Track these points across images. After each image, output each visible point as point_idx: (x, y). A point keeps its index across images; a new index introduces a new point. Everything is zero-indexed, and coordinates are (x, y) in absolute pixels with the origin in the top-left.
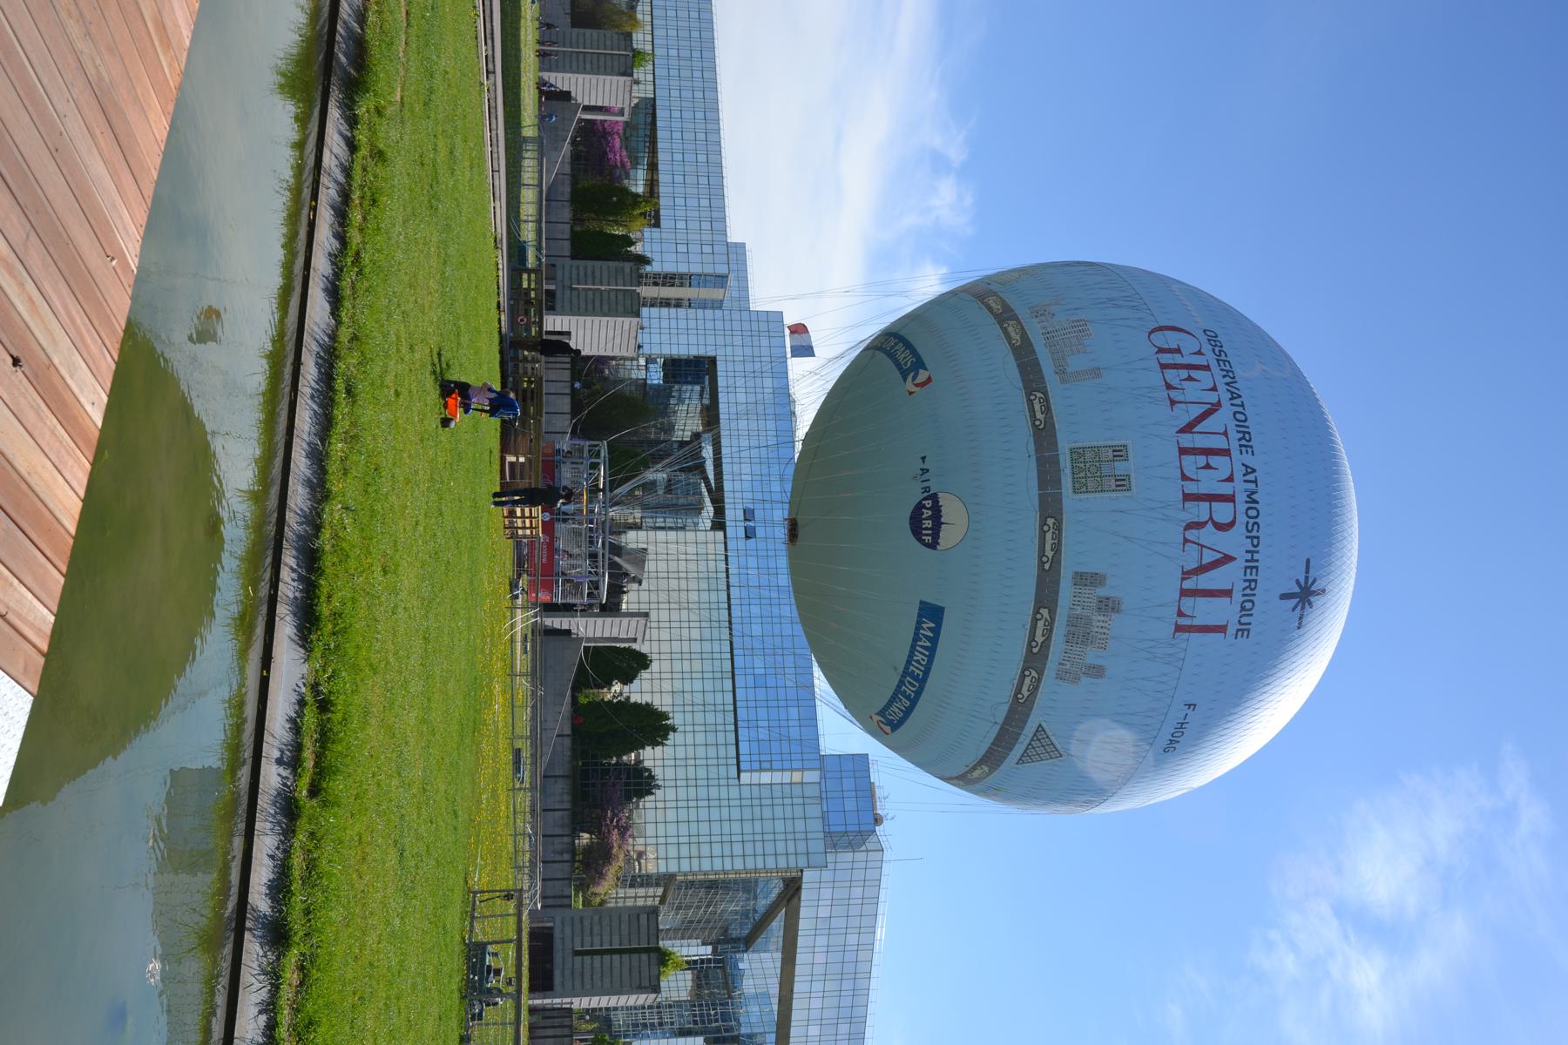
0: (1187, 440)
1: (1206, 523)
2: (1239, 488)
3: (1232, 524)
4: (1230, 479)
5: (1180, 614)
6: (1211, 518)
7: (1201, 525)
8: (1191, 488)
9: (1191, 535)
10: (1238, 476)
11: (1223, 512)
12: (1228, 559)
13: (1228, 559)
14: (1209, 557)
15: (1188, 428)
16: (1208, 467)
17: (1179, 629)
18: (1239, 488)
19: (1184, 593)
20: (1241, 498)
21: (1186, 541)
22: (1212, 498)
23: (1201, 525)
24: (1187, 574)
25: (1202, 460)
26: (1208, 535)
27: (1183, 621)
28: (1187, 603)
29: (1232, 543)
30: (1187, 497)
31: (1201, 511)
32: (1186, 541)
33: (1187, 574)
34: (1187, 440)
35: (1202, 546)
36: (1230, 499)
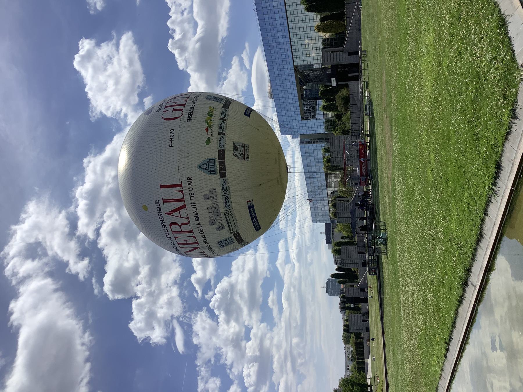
0: (196, 246)
1: (181, 225)
2: (172, 236)
3: (171, 225)
4: (176, 238)
5: (182, 192)
6: (180, 226)
7: (182, 224)
8: (191, 234)
9: (186, 221)
10: (173, 239)
11: (175, 228)
12: (170, 213)
13: (170, 213)
14: (177, 214)
15: (196, 248)
16: (186, 240)
17: (180, 185)
18: (172, 236)
19: (182, 200)
20: (170, 232)
21: (188, 218)
22: (181, 232)
23: (182, 224)
24: (184, 206)
25: (188, 242)
26: (180, 221)
27: (179, 189)
28: (179, 196)
29: (168, 219)
30: (191, 231)
31: (185, 228)
32: (188, 218)
33: (184, 206)
34: (196, 246)
35: (181, 217)
36: (174, 232)
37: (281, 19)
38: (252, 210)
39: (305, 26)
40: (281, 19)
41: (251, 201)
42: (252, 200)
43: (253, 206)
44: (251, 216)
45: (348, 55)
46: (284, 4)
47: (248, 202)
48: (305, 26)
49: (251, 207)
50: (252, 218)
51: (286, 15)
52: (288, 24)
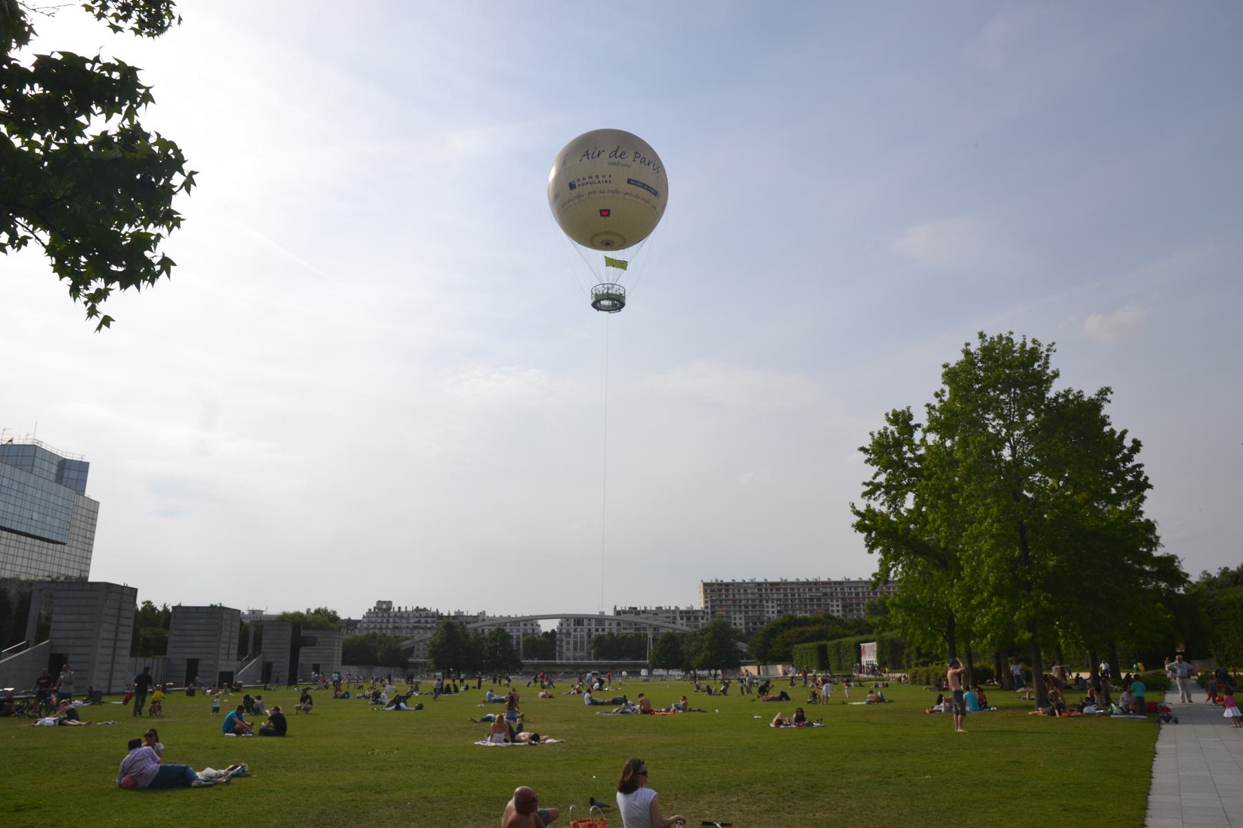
43: (655, 195)
50: (649, 187)
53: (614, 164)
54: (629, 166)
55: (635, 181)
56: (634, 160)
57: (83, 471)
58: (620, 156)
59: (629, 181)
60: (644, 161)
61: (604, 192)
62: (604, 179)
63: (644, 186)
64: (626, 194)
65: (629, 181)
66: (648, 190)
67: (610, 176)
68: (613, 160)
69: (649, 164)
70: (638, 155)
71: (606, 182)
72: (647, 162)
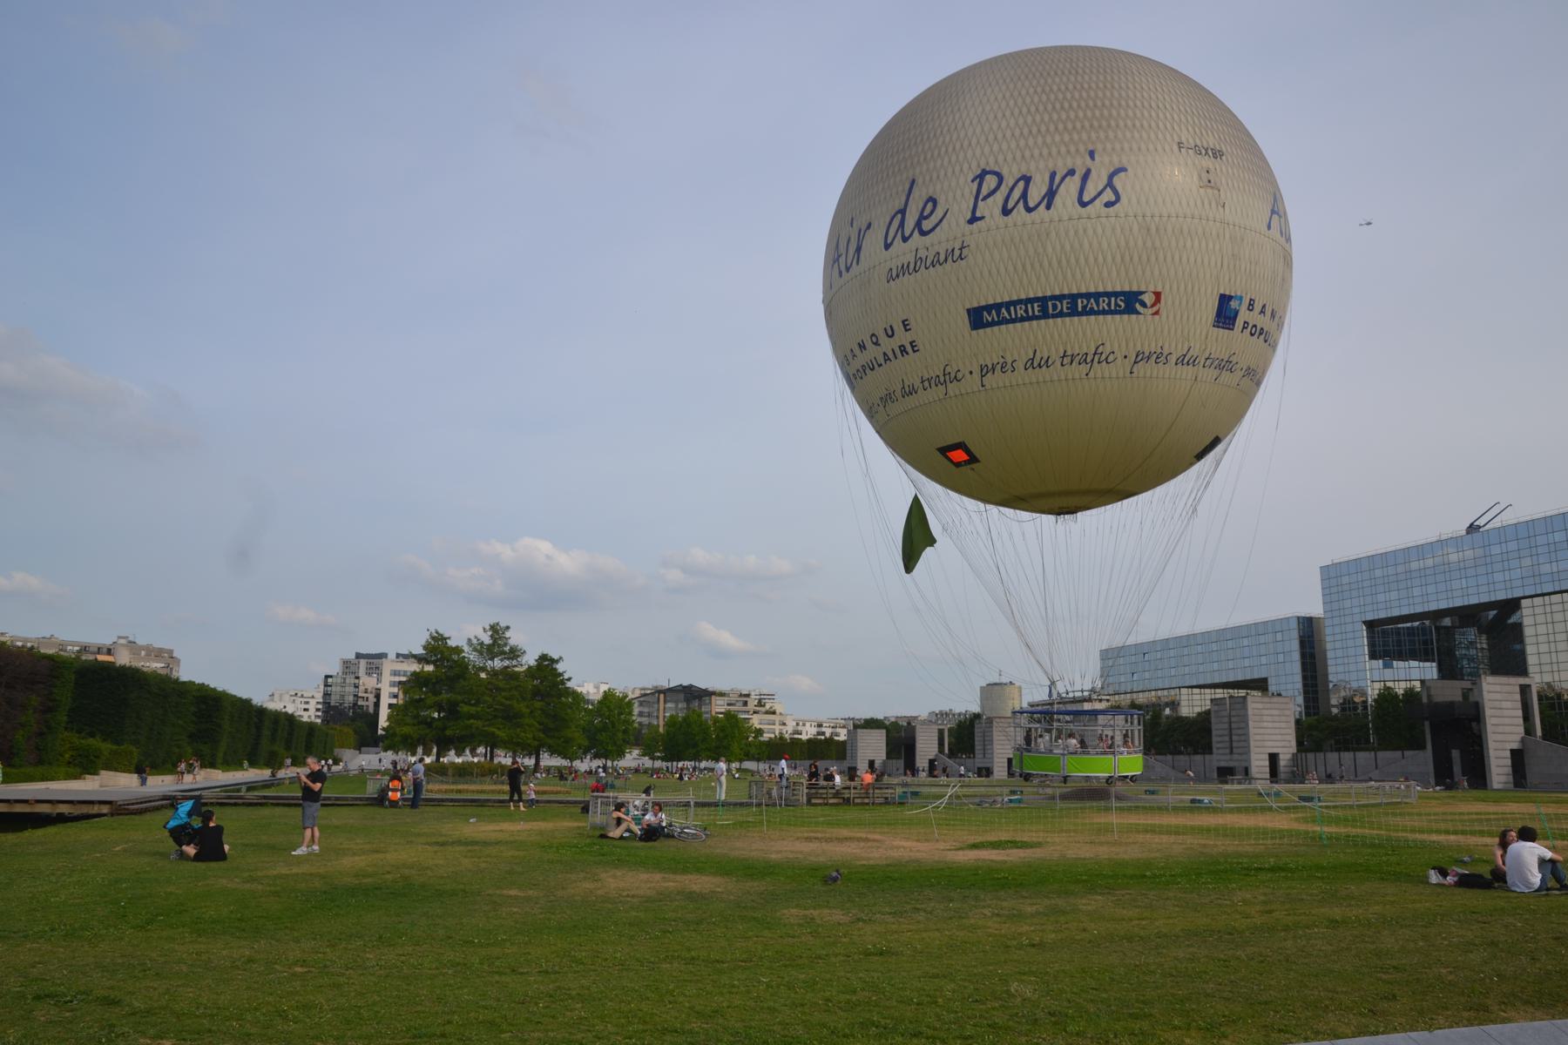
37: (1508, 586)
38: (1116, 304)
39: (1541, 639)
40: (1508, 586)
41: (1155, 309)
42: (1157, 313)
43: (1130, 310)
44: (1088, 296)
45: (1511, 750)
46: (1545, 591)
47: (1158, 295)
48: (1541, 639)
49: (1130, 302)
50: (1073, 298)
51: (1549, 591)
52: (1543, 595)
53: (904, 270)
54: (957, 254)
55: (997, 307)
56: (973, 220)
57: (1327, 603)
58: (918, 224)
59: (978, 318)
60: (1024, 196)
61: (912, 391)
62: (894, 343)
63: (1045, 307)
64: (985, 370)
65: (978, 318)
66: (1074, 312)
67: (905, 324)
68: (902, 252)
69: (1051, 195)
70: (991, 182)
71: (903, 350)
72: (1036, 192)
